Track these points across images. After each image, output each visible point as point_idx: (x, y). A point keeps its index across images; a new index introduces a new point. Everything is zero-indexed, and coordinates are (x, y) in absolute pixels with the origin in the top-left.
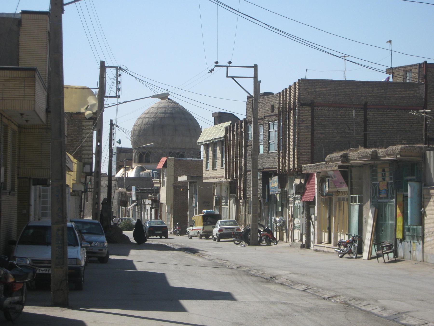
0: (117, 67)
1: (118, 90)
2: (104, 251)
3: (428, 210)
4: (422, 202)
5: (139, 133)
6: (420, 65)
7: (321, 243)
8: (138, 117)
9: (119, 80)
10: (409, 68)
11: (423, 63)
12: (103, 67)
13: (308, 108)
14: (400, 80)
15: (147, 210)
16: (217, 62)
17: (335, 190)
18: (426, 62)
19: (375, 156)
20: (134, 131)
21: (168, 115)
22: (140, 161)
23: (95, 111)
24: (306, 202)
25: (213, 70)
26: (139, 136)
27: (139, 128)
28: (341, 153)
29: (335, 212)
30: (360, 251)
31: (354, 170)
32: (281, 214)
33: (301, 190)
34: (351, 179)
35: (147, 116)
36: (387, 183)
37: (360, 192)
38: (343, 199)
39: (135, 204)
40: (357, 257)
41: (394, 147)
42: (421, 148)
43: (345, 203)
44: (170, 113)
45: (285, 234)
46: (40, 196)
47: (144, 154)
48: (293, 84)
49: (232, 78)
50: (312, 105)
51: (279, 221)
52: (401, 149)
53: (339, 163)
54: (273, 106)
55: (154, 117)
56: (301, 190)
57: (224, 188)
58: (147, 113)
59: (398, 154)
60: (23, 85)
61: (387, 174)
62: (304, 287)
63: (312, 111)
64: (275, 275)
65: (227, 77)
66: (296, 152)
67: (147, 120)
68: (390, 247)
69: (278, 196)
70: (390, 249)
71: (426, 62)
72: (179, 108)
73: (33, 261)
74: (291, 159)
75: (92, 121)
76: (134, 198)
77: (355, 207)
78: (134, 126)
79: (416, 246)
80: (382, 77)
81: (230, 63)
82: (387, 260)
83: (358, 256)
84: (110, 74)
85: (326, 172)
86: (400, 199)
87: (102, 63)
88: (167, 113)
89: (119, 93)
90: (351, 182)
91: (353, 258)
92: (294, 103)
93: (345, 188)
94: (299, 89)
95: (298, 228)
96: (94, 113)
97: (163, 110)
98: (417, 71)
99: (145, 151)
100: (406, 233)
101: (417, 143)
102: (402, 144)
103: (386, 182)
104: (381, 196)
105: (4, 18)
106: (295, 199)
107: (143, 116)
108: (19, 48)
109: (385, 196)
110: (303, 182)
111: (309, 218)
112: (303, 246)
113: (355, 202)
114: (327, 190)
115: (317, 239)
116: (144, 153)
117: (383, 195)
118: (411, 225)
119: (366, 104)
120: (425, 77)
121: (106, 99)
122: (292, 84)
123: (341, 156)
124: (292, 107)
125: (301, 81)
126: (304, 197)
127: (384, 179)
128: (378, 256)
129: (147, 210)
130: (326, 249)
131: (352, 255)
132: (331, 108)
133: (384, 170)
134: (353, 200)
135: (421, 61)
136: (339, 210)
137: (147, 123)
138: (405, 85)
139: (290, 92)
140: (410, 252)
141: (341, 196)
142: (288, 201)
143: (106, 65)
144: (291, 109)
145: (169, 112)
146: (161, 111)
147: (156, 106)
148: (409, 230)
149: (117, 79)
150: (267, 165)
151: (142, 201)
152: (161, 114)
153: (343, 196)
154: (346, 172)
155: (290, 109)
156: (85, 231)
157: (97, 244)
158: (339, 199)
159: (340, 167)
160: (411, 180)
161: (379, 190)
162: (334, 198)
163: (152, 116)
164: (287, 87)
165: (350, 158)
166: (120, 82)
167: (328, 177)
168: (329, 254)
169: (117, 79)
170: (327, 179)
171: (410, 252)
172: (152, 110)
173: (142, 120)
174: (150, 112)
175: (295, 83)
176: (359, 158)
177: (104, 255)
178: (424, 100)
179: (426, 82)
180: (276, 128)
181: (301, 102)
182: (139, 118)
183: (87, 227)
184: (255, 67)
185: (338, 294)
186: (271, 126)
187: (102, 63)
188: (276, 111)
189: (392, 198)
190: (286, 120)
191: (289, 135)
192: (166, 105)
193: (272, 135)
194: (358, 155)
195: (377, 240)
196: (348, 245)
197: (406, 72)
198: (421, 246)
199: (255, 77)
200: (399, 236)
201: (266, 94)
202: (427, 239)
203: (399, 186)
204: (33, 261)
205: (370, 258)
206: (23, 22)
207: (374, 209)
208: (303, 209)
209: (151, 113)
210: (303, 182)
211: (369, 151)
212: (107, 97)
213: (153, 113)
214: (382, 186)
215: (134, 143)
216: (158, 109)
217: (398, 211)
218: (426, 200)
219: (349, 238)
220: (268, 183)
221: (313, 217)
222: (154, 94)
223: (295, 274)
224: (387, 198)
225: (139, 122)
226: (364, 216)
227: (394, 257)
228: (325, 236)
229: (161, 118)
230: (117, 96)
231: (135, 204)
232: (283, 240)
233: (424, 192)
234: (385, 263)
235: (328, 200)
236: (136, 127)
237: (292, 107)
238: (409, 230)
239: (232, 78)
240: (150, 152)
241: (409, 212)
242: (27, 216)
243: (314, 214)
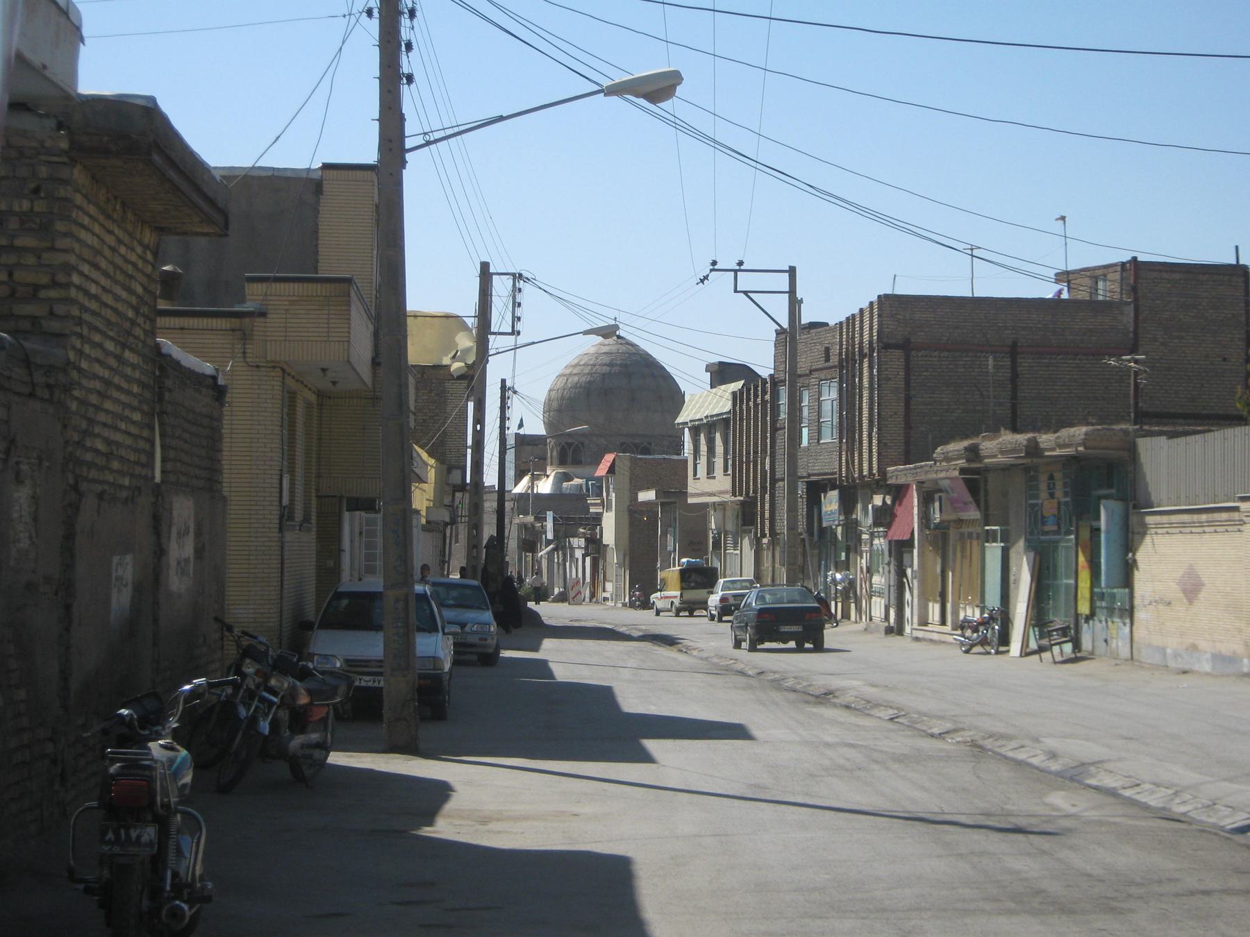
0: (513, 275)
1: (516, 319)
2: (489, 641)
3: (1141, 556)
4: (1129, 540)
6: (1123, 264)
7: (926, 624)
9: (518, 300)
10: (1100, 272)
11: (1129, 262)
12: (486, 274)
13: (898, 353)
14: (1083, 295)
16: (714, 263)
17: (953, 517)
18: (1135, 259)
19: (1033, 450)
22: (562, 462)
23: (470, 362)
24: (898, 542)
25: (706, 278)
26: (559, 411)
28: (966, 443)
29: (954, 561)
30: (1004, 639)
31: (991, 477)
32: (846, 566)
33: (884, 517)
34: (986, 495)
36: (1059, 503)
37: (1004, 522)
38: (970, 535)
40: (997, 653)
41: (1072, 430)
42: (1126, 432)
43: (975, 543)
44: (621, 365)
45: (853, 606)
46: (361, 533)
48: (867, 304)
49: (746, 293)
50: (906, 346)
51: (842, 580)
52: (1086, 434)
53: (961, 463)
54: (827, 350)
56: (884, 517)
57: (729, 513)
58: (577, 365)
59: (1079, 445)
60: (108, 405)
61: (1059, 484)
62: (891, 712)
63: (907, 360)
64: (833, 688)
65: (736, 291)
66: (875, 442)
67: (576, 378)
68: (1064, 631)
69: (839, 529)
70: (1065, 636)
71: (1135, 259)
73: (347, 661)
74: (865, 455)
75: (464, 383)
76: (550, 536)
77: (993, 551)
79: (1119, 628)
80: (1048, 291)
81: (741, 263)
82: (1058, 658)
83: (1002, 649)
84: (501, 287)
85: (935, 481)
86: (1085, 534)
87: (485, 266)
89: (519, 327)
90: (986, 501)
91: (989, 653)
92: (871, 342)
93: (974, 514)
94: (879, 316)
95: (880, 594)
96: (468, 366)
97: (606, 359)
98: (1117, 276)
99: (570, 441)
100: (1098, 604)
101: (1118, 422)
102: (1088, 424)
103: (1055, 501)
104: (1046, 528)
105: (288, 179)
106: (872, 535)
107: (568, 371)
108: (317, 239)
109: (1055, 528)
110: (889, 502)
111: (901, 573)
112: (889, 631)
113: (995, 541)
114: (937, 517)
115: (919, 617)
116: (570, 445)
117: (1050, 527)
118: (1107, 587)
119: (1014, 346)
120: (1134, 289)
121: (491, 338)
122: (865, 305)
123: (966, 449)
124: (866, 350)
125: (884, 299)
126: (890, 533)
127: (1052, 496)
128: (1041, 649)
130: (935, 637)
131: (988, 648)
132: (946, 354)
133: (1051, 477)
134: (990, 537)
135: (1126, 257)
136: (962, 557)
137: (575, 386)
138: (1093, 306)
139: (862, 322)
140: (1106, 641)
141: (965, 530)
142: (860, 540)
143: (492, 270)
144: (865, 356)
147: (592, 350)
148: (1102, 596)
149: (514, 298)
150: (817, 468)
153: (970, 530)
154: (975, 480)
155: (862, 356)
156: (451, 602)
157: (475, 628)
158: (962, 535)
159: (963, 471)
160: (1106, 497)
161: (1043, 517)
162: (953, 534)
163: (586, 371)
164: (856, 311)
165: (983, 453)
166: (519, 305)
167: (940, 491)
168: (942, 647)
169: (514, 298)
170: (937, 496)
171: (1106, 641)
175: (871, 304)
176: (1002, 452)
177: (491, 650)
178: (1131, 335)
179: (1136, 300)
180: (834, 394)
181: (885, 340)
183: (454, 593)
184: (792, 271)
185: (961, 726)
186: (825, 389)
187: (485, 266)
188: (834, 360)
189: (1068, 533)
190: (854, 376)
191: (861, 408)
192: (614, 348)
193: (827, 407)
194: (999, 446)
195: (1039, 617)
196: (981, 629)
197: (1096, 279)
198: (1127, 629)
199: (792, 292)
200: (1084, 608)
201: (813, 325)
202: (1140, 615)
203: (1083, 509)
204: (347, 661)
205: (1026, 653)
206: (326, 187)
207: (1032, 555)
208: (890, 555)
210: (889, 502)
211: (1022, 438)
212: (495, 333)
214: (1049, 508)
215: (549, 424)
217: (1081, 559)
218: (1136, 536)
219: (982, 613)
220: (818, 503)
221: (909, 571)
222: (589, 327)
223: (873, 686)
224: (1058, 532)
225: (560, 384)
226: (1013, 569)
227: (1074, 652)
228: (934, 610)
230: (515, 332)
232: (849, 618)
233: (1134, 519)
234: (1055, 663)
235: (940, 538)
237: (866, 350)
238: (1102, 596)
239: (746, 293)
240: (582, 444)
241: (1103, 560)
242: (336, 571)
243: (911, 566)
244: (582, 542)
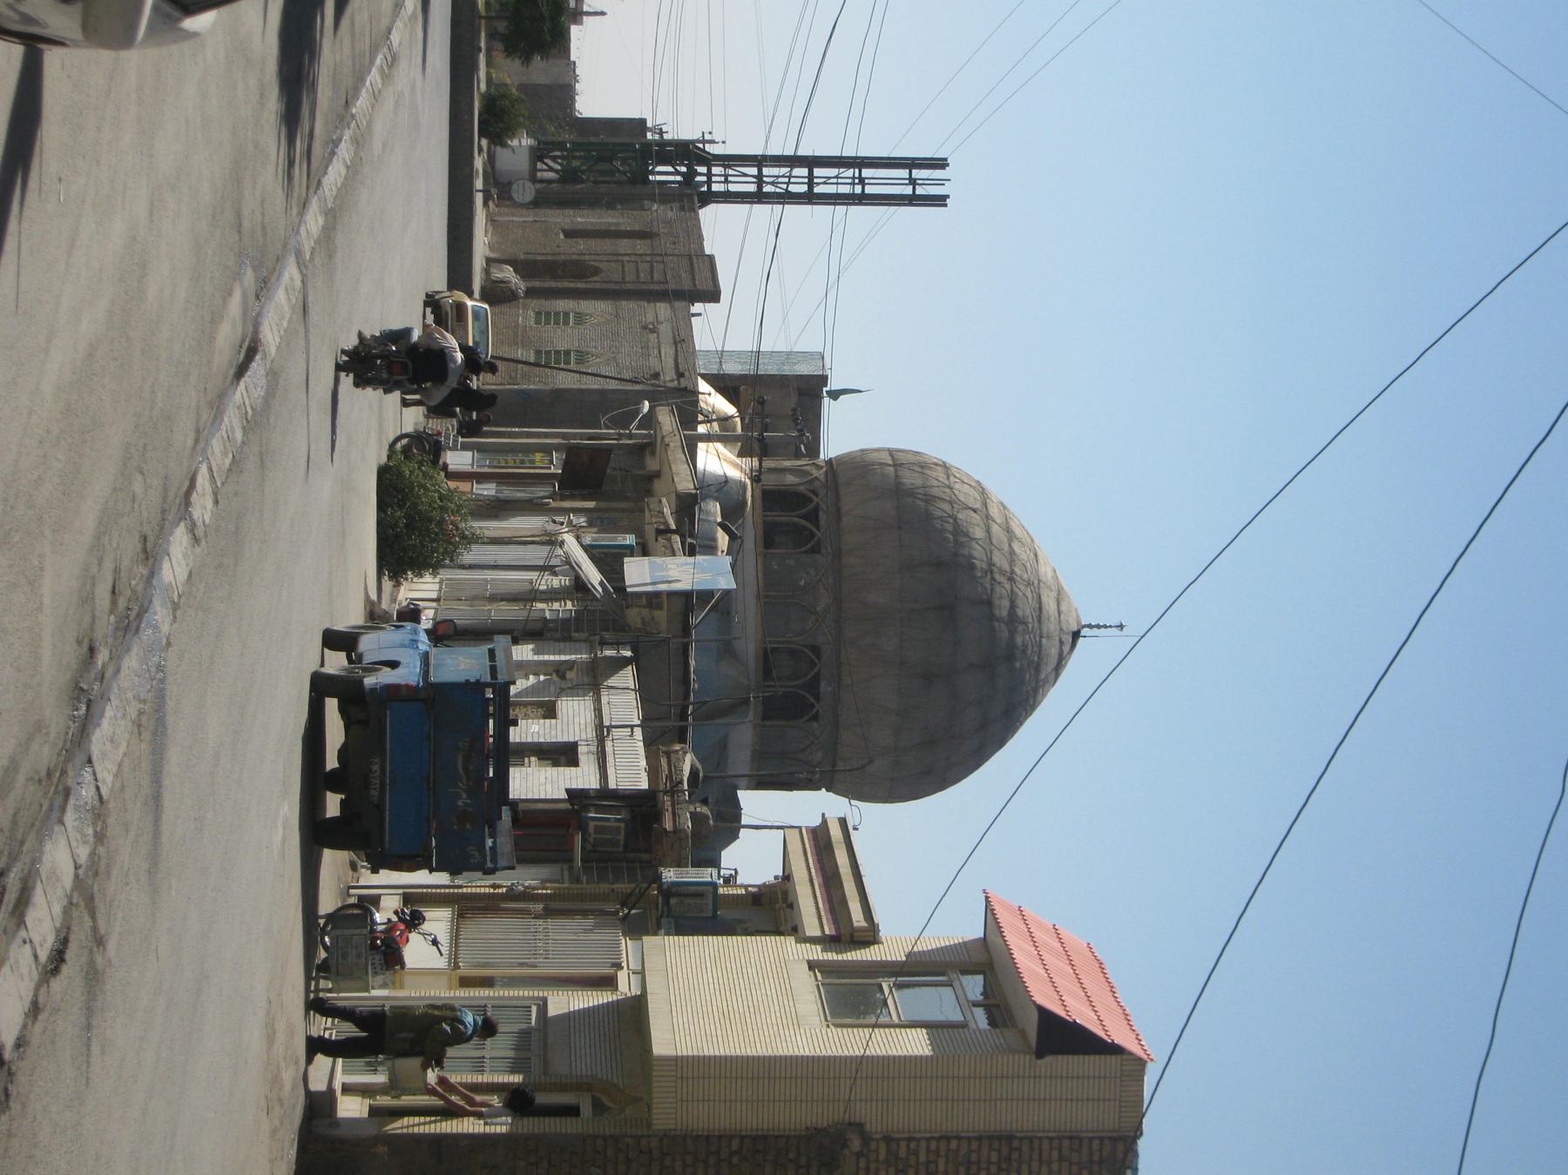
5: (911, 493)
8: (985, 484)
15: (550, 712)
20: (922, 465)
21: (1005, 634)
22: (772, 498)
26: (899, 492)
27: (935, 492)
35: (995, 528)
39: (593, 575)
47: (804, 517)
55: (991, 564)
58: (1008, 530)
67: (978, 533)
72: (1035, 691)
76: (639, 573)
78: (945, 466)
88: (1012, 632)
97: (1025, 609)
99: (822, 517)
107: (994, 511)
116: (813, 516)
129: (550, 712)
137: (960, 532)
145: (1019, 640)
146: (1019, 603)
147: (1045, 571)
151: (617, 644)
152: (1006, 603)
163: (999, 560)
172: (1023, 554)
173: (978, 505)
174: (1016, 546)
182: (983, 492)
192: (1051, 626)
209: (1012, 552)
213: (1012, 562)
215: (857, 467)
216: (1029, 583)
225: (965, 494)
229: (990, 603)
231: (593, 575)
240: (815, 550)
244: (630, 769)
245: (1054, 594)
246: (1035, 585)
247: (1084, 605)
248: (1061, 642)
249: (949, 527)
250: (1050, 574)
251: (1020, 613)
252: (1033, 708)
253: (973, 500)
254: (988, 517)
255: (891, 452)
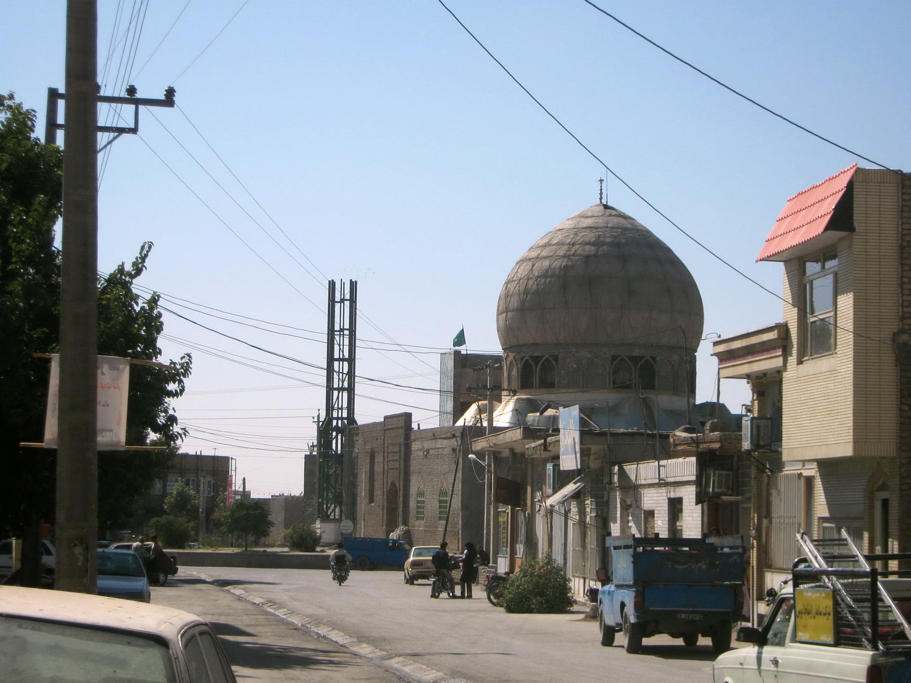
5: (523, 303)
20: (506, 296)
21: (605, 248)
22: (525, 383)
27: (522, 288)
35: (544, 254)
44: (611, 244)
47: (537, 364)
55: (564, 256)
58: (545, 246)
67: (546, 263)
72: (638, 230)
78: (507, 283)
97: (591, 236)
99: (536, 354)
107: (534, 254)
116: (536, 359)
137: (545, 274)
145: (609, 240)
146: (587, 240)
147: (569, 224)
152: (587, 248)
163: (561, 253)
173: (530, 264)
174: (554, 242)
182: (522, 261)
192: (601, 222)
209: (557, 244)
213: (563, 244)
215: (507, 333)
216: (576, 234)
225: (523, 271)
229: (587, 257)
236: (511, 286)
240: (556, 358)
245: (582, 219)
246: (576, 231)
247: (588, 202)
248: (610, 215)
249: (543, 280)
250: (570, 222)
251: (593, 239)
252: (648, 232)
253: (527, 266)
254: (537, 258)
255: (499, 314)
